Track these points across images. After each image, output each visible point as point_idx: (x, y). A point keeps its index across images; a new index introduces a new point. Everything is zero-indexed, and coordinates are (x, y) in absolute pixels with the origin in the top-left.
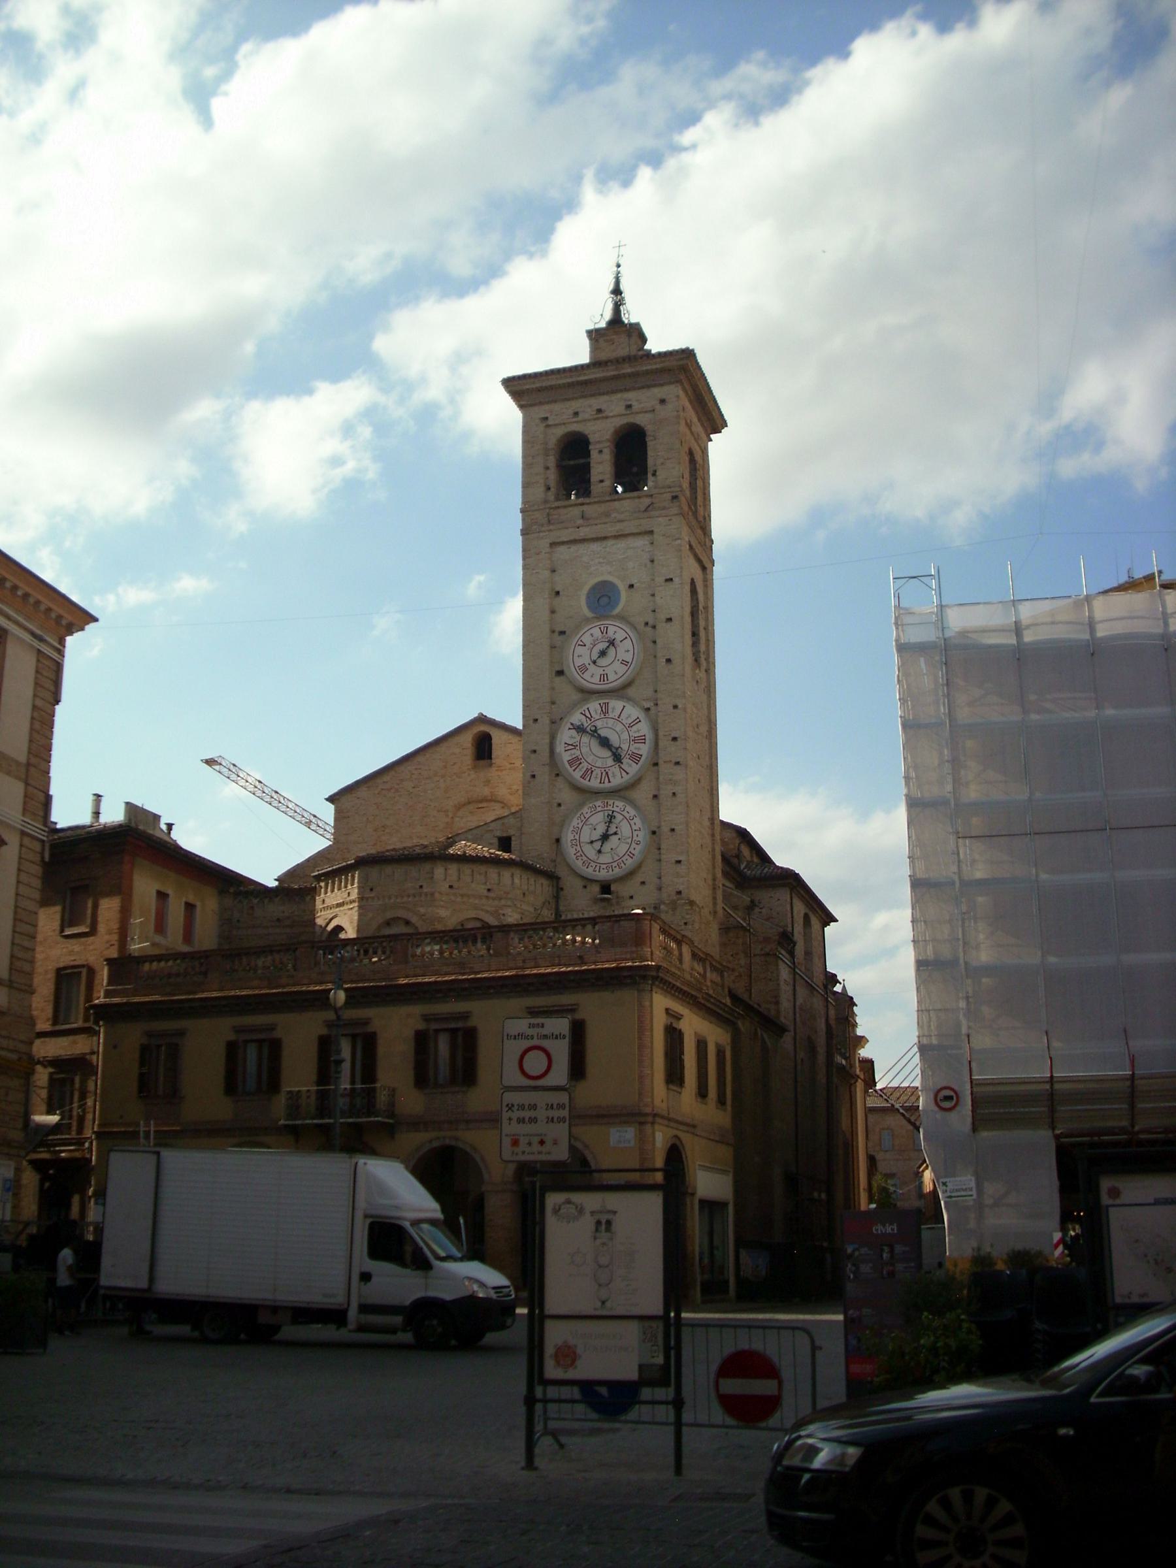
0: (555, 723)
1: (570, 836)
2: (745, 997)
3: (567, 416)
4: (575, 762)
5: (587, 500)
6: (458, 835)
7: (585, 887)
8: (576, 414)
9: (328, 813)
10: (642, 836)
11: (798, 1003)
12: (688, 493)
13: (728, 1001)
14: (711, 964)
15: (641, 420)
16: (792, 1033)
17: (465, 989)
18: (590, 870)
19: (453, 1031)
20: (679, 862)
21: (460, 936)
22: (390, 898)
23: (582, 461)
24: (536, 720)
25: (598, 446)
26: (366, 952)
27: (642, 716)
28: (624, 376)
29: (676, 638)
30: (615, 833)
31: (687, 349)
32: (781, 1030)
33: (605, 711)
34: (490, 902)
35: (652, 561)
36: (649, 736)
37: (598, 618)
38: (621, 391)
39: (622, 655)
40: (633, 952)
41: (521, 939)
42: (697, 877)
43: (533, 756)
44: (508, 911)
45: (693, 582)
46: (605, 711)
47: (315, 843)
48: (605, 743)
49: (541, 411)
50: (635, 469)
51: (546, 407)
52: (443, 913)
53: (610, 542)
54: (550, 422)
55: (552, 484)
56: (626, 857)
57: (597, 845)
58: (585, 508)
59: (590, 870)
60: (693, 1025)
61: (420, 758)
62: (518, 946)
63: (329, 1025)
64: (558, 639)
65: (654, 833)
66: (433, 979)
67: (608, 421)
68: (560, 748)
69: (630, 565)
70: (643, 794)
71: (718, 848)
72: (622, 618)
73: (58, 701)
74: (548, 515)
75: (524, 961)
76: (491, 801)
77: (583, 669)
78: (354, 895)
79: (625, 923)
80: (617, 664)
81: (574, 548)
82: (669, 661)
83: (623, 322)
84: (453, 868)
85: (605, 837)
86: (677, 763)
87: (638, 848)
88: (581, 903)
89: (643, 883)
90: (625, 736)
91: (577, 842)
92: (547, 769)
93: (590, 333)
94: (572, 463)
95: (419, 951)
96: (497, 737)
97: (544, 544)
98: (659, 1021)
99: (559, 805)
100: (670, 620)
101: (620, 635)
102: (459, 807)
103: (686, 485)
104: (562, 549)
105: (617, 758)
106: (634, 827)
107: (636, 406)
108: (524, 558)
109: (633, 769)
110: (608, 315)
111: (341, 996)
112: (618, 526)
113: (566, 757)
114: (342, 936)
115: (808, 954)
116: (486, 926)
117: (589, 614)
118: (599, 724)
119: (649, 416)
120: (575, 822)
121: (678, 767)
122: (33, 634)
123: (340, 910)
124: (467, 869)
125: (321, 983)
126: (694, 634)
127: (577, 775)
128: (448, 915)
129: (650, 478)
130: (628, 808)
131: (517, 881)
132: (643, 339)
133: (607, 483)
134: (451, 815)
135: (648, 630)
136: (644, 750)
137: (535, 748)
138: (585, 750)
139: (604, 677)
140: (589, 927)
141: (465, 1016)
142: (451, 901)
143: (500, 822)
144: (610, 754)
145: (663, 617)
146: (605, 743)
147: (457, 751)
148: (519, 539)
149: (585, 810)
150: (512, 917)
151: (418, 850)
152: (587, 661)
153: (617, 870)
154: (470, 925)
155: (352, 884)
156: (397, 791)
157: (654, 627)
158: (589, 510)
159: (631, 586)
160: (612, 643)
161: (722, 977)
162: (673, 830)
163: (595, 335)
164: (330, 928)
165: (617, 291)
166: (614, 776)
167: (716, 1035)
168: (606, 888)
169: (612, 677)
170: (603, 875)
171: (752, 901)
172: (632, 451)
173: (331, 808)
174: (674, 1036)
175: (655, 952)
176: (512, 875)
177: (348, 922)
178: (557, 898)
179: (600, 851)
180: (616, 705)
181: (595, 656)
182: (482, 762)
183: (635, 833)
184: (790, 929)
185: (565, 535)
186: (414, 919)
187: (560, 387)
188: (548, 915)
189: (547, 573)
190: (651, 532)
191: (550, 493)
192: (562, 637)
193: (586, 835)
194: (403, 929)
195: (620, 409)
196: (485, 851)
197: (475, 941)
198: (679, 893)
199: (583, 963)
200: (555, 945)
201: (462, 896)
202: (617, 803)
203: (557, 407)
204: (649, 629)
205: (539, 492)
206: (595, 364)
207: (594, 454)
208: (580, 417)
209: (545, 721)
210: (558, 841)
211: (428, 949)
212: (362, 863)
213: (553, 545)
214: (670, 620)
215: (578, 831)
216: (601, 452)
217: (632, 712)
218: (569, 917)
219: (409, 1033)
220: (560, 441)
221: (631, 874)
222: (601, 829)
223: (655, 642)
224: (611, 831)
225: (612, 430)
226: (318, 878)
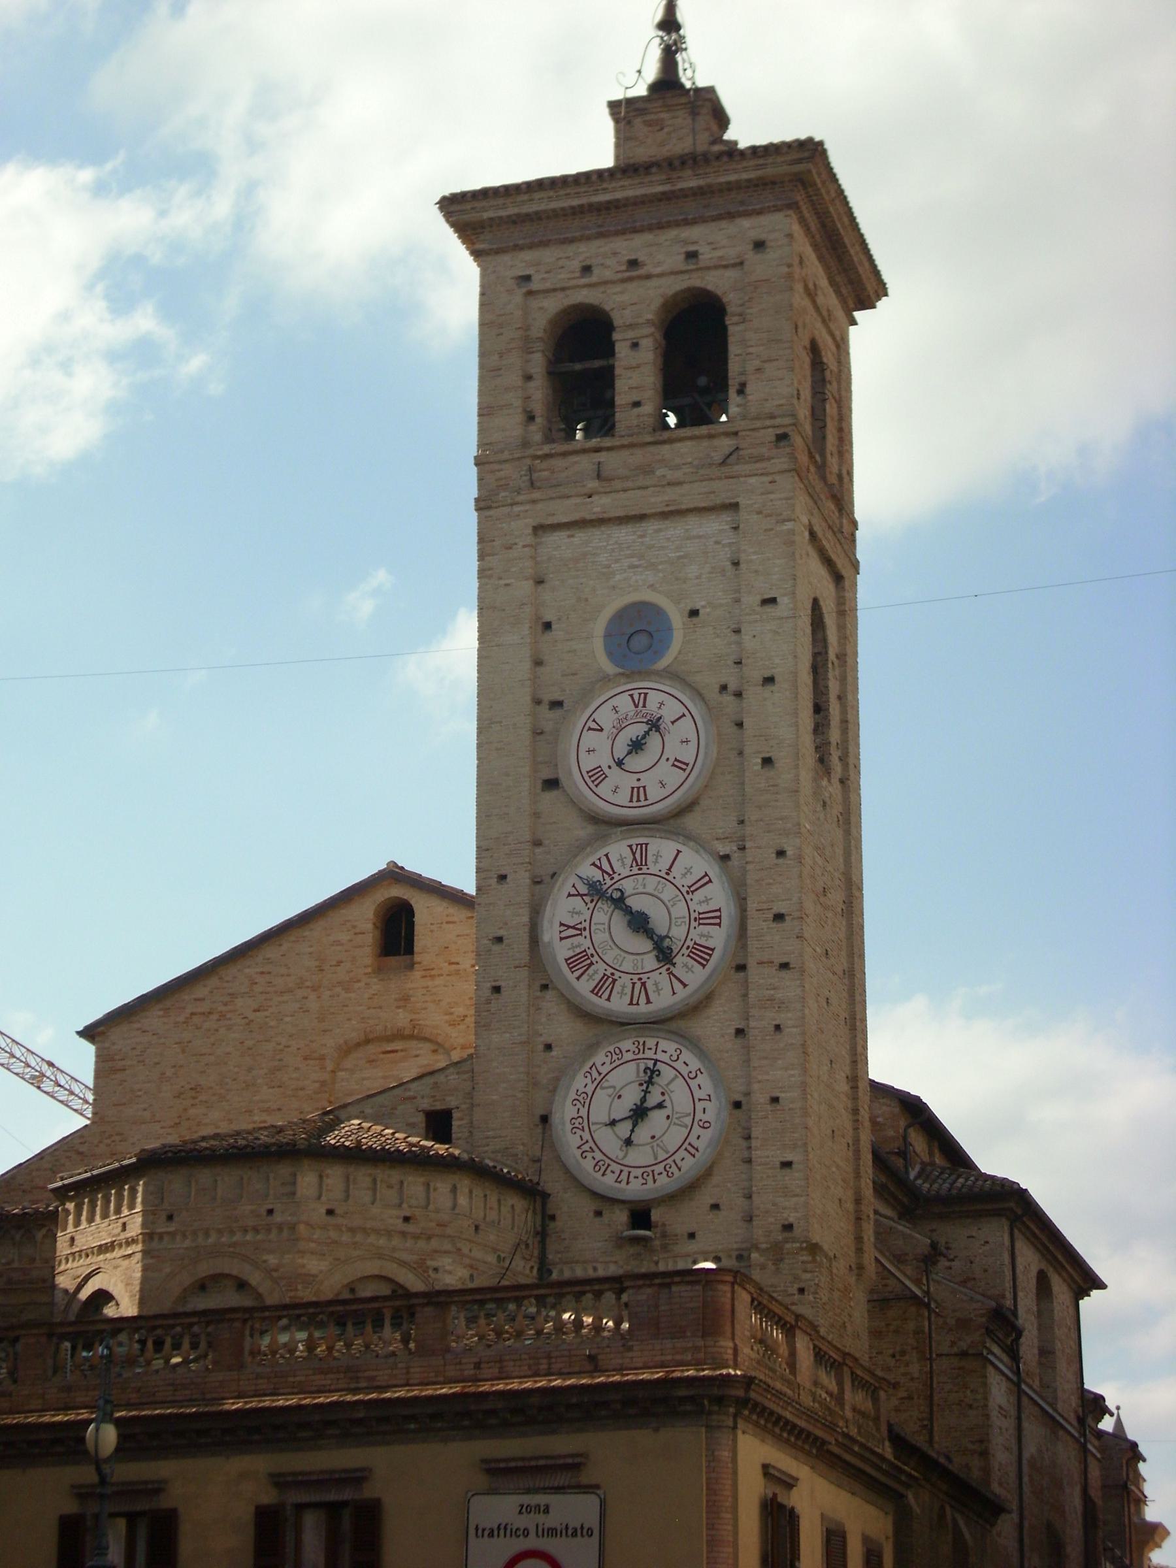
0: (542, 882)
1: (570, 1111)
2: (920, 1441)
3: (567, 274)
4: (581, 961)
5: (607, 442)
6: (345, 1106)
7: (598, 1214)
8: (587, 269)
9: (82, 1062)
10: (712, 1111)
11: (1026, 1455)
12: (808, 428)
13: (888, 1451)
14: (854, 1377)
15: (716, 282)
16: (1015, 1516)
17: (359, 1422)
18: (610, 1179)
19: (333, 1509)
20: (787, 1165)
21: (347, 1313)
22: (207, 1234)
23: (597, 364)
24: (503, 878)
25: (631, 334)
26: (159, 1345)
27: (714, 871)
28: (684, 194)
29: (782, 719)
30: (660, 1106)
31: (810, 140)
32: (995, 1509)
33: (640, 860)
34: (409, 1243)
35: (736, 564)
36: (729, 912)
37: (630, 675)
38: (677, 224)
39: (674, 750)
40: (696, 1349)
41: (472, 1320)
42: (825, 1199)
43: (496, 948)
44: (446, 1262)
45: (816, 602)
46: (640, 860)
47: (55, 1122)
48: (639, 923)
49: (519, 263)
50: (702, 381)
51: (527, 255)
52: (314, 1265)
53: (650, 526)
54: (535, 285)
55: (538, 408)
56: (682, 1153)
57: (624, 1129)
58: (602, 457)
59: (610, 1179)
60: (817, 1498)
61: (270, 952)
62: (464, 1334)
63: (82, 1494)
64: (548, 717)
65: (737, 1105)
66: (293, 1401)
67: (654, 282)
68: (550, 933)
69: (693, 570)
70: (714, 1028)
71: (866, 1138)
72: (672, 675)
74: (531, 470)
75: (477, 1366)
76: (412, 1037)
77: (597, 776)
78: (135, 1227)
79: (680, 1290)
80: (664, 768)
81: (580, 536)
82: (767, 761)
83: (682, 86)
84: (335, 1175)
85: (639, 1113)
86: (785, 966)
87: (707, 1135)
88: (590, 1247)
89: (715, 1207)
90: (680, 910)
91: (582, 1123)
92: (524, 973)
93: (614, 107)
94: (578, 367)
95: (266, 1341)
96: (425, 911)
97: (521, 528)
98: (750, 1491)
99: (548, 1047)
100: (769, 680)
101: (671, 710)
102: (347, 1050)
103: (803, 412)
104: (559, 537)
105: (665, 955)
106: (698, 1094)
107: (707, 256)
108: (482, 556)
109: (695, 976)
110: (652, 72)
111: (109, 1435)
112: (671, 494)
113: (562, 951)
114: (110, 1311)
115: (1046, 1352)
116: (400, 1292)
117: (610, 668)
118: (628, 886)
119: (731, 274)
120: (580, 1082)
121: (784, 974)
123: (105, 1260)
124: (362, 1175)
125: (66, 1408)
126: (818, 709)
127: (584, 987)
128: (323, 1268)
130: (687, 1056)
131: (463, 1201)
132: (721, 119)
133: (648, 408)
134: (330, 1066)
135: (727, 701)
136: (718, 938)
137: (501, 933)
138: (600, 937)
139: (638, 793)
140: (609, 1297)
141: (357, 1478)
142: (330, 1238)
143: (430, 1080)
144: (648, 945)
145: (757, 675)
146: (639, 923)
147: (344, 937)
148: (470, 520)
149: (600, 1058)
150: (453, 1275)
151: (264, 1138)
152: (605, 760)
153: (663, 1180)
154: (367, 1291)
155: (132, 1206)
156: (222, 1016)
157: (738, 695)
158: (613, 461)
159: (694, 613)
160: (655, 725)
161: (875, 1400)
162: (775, 1100)
163: (624, 112)
164: (84, 1295)
165: (669, 23)
166: (658, 991)
167: (863, 1519)
168: (640, 1216)
169: (654, 793)
170: (635, 1189)
171: (934, 1246)
172: (696, 342)
173: (88, 1051)
174: (779, 1521)
175: (742, 1347)
176: (454, 1190)
177: (122, 1284)
178: (542, 1235)
179: (628, 1142)
180: (662, 848)
181: (621, 750)
182: (393, 961)
183: (700, 1106)
184: (1009, 1303)
185: (563, 511)
186: (255, 1278)
187: (555, 214)
188: (524, 1271)
189: (528, 585)
190: (734, 506)
191: (533, 428)
192: (558, 713)
193: (601, 1109)
194: (230, 1299)
195: (675, 260)
196: (401, 1139)
197: (378, 1324)
198: (788, 1227)
199: (597, 1369)
200: (539, 1332)
201: (352, 1230)
202: (664, 1044)
203: (548, 255)
204: (728, 699)
205: (511, 425)
206: (625, 169)
207: (622, 350)
208: (596, 275)
209: (521, 879)
210: (545, 1119)
211: (284, 1338)
212: (152, 1163)
214: (769, 680)
215: (585, 1099)
216: (635, 345)
217: (694, 863)
218: (567, 1274)
219: (244, 1513)
220: (554, 322)
221: (689, 1189)
222: (632, 1097)
223: (740, 725)
224: (652, 1101)
225: (657, 303)
226: (62, 1194)
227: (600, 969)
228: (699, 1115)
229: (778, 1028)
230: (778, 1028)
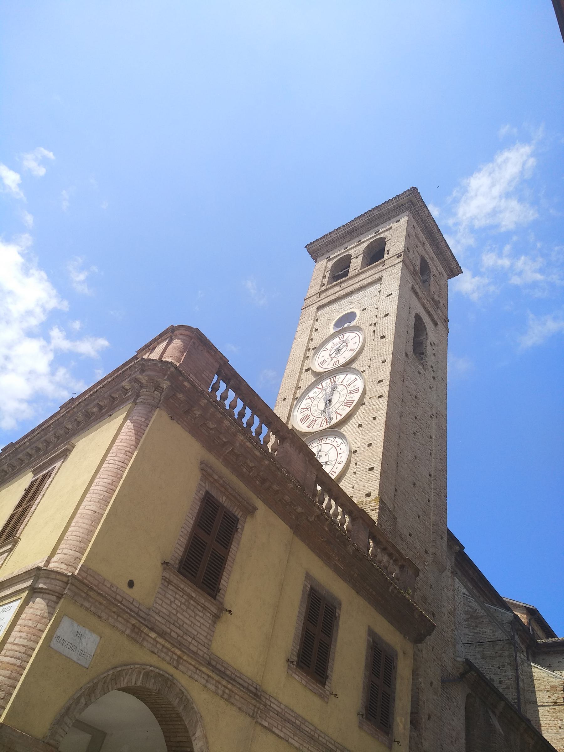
20: (371, 469)
100: (386, 315)
162: (370, 445)
183: (339, 456)
214: (386, 315)
216: (357, 257)
227: (312, 418)
228: (339, 459)
230: (375, 418)
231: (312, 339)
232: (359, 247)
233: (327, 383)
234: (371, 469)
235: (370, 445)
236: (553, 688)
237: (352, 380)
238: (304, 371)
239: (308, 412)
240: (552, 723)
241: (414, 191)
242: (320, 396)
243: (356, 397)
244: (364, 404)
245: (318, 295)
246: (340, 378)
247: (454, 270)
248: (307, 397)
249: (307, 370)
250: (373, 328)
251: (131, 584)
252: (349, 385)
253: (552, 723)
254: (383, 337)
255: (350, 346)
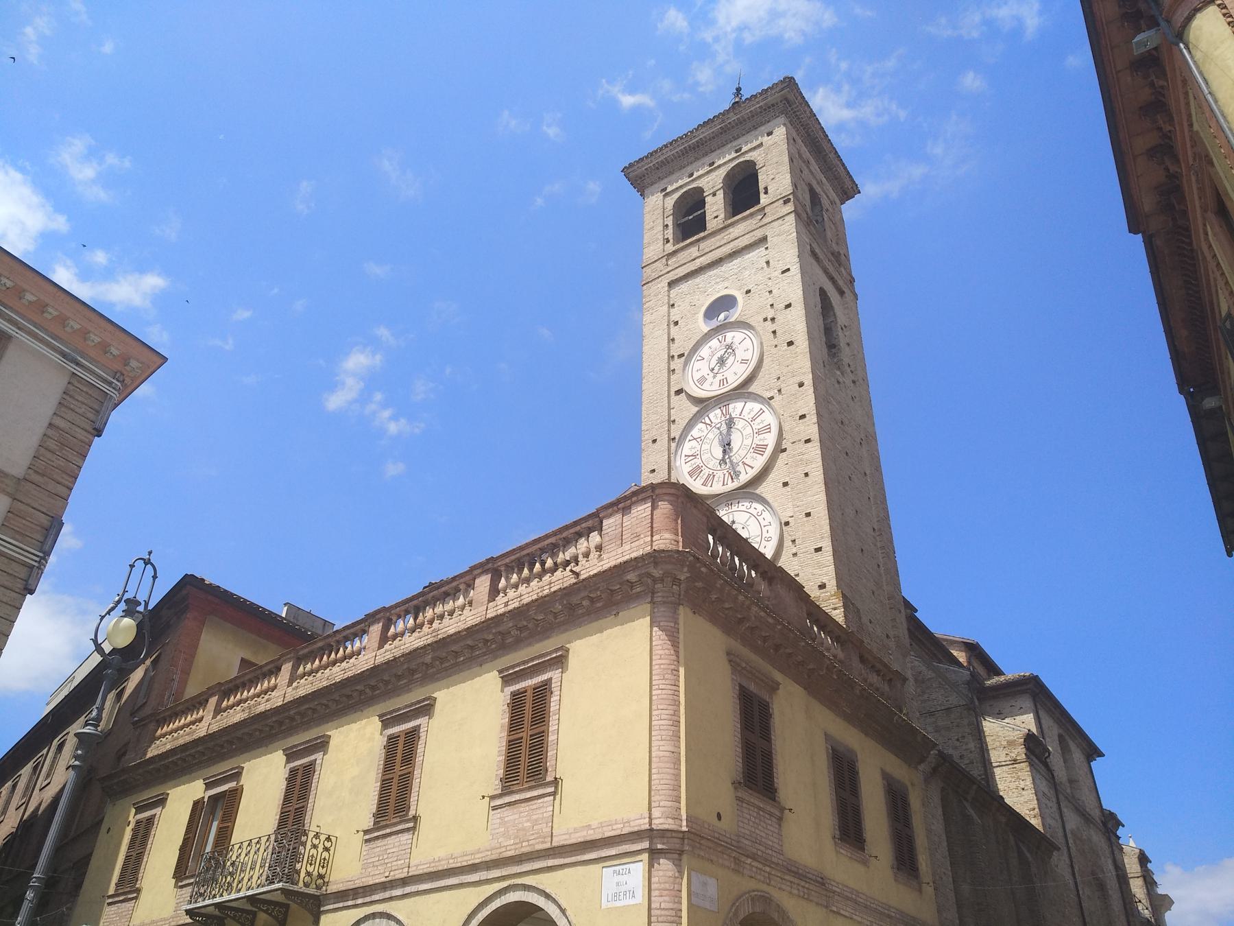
5: (702, 234)
20: (818, 550)
24: (654, 441)
64: (677, 364)
73: (99, 433)
100: (788, 306)
122: (64, 355)
129: (762, 196)
130: (755, 505)
139: (723, 382)
152: (705, 371)
159: (748, 292)
162: (808, 515)
183: (765, 530)
190: (764, 239)
213: (671, 284)
214: (788, 306)
216: (714, 194)
227: (706, 472)
229: (806, 475)
230: (806, 475)
231: (673, 340)
232: (714, 175)
233: (716, 415)
234: (818, 550)
235: (808, 515)
236: (1011, 743)
237: (756, 411)
238: (672, 393)
239: (698, 461)
240: (1013, 785)
241: (790, 82)
242: (711, 436)
243: (770, 440)
244: (785, 450)
245: (664, 260)
246: (736, 407)
247: (848, 190)
248: (689, 437)
249: (679, 392)
250: (770, 326)
251: (719, 816)
252: (753, 419)
253: (1013, 785)
254: (790, 344)
255: (740, 354)
